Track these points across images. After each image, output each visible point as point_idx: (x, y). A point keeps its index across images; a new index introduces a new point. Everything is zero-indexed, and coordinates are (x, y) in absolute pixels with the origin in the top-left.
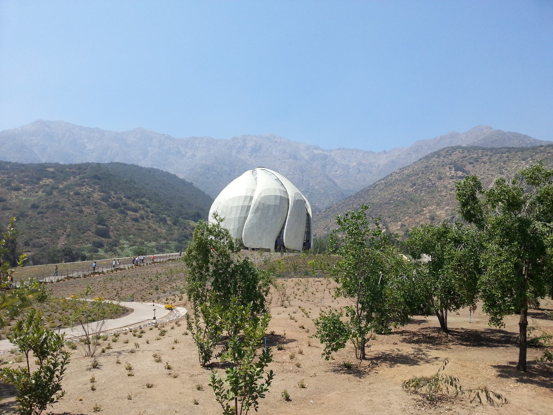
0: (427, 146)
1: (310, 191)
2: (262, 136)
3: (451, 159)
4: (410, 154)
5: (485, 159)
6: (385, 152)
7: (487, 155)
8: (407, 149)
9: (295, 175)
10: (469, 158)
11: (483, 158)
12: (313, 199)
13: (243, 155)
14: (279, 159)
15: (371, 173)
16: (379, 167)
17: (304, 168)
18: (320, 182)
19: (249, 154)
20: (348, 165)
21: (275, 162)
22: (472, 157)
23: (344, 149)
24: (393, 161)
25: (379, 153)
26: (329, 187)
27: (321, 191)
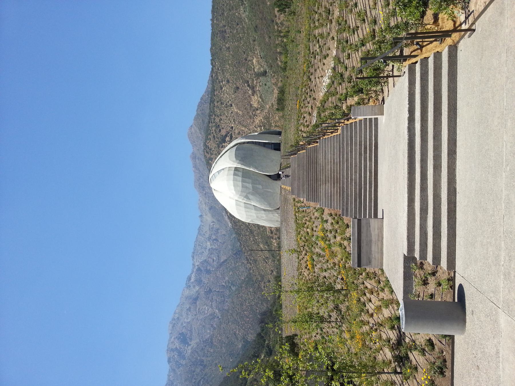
0: (200, 179)
1: (230, 285)
2: (171, 332)
3: (215, 149)
4: (205, 194)
5: (217, 120)
6: (201, 216)
7: (215, 119)
8: (200, 196)
9: (213, 299)
10: (216, 133)
11: (216, 121)
12: (238, 282)
13: (186, 352)
14: (196, 315)
15: (218, 229)
16: (214, 222)
17: (207, 290)
18: (222, 275)
19: (187, 345)
20: (209, 250)
21: (198, 319)
22: (215, 130)
23: (194, 253)
24: (210, 209)
25: (201, 221)
26: (228, 266)
27: (230, 274)
